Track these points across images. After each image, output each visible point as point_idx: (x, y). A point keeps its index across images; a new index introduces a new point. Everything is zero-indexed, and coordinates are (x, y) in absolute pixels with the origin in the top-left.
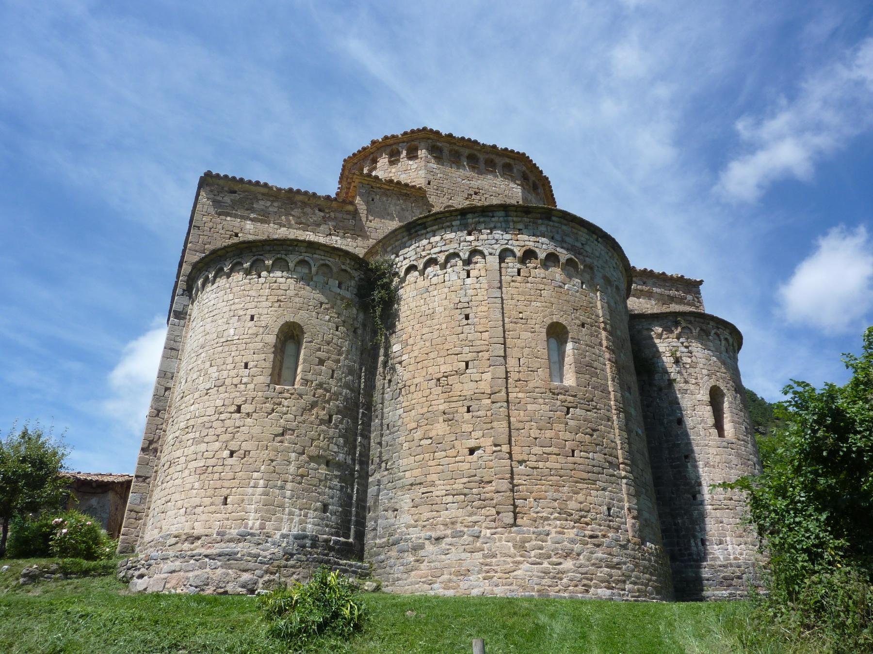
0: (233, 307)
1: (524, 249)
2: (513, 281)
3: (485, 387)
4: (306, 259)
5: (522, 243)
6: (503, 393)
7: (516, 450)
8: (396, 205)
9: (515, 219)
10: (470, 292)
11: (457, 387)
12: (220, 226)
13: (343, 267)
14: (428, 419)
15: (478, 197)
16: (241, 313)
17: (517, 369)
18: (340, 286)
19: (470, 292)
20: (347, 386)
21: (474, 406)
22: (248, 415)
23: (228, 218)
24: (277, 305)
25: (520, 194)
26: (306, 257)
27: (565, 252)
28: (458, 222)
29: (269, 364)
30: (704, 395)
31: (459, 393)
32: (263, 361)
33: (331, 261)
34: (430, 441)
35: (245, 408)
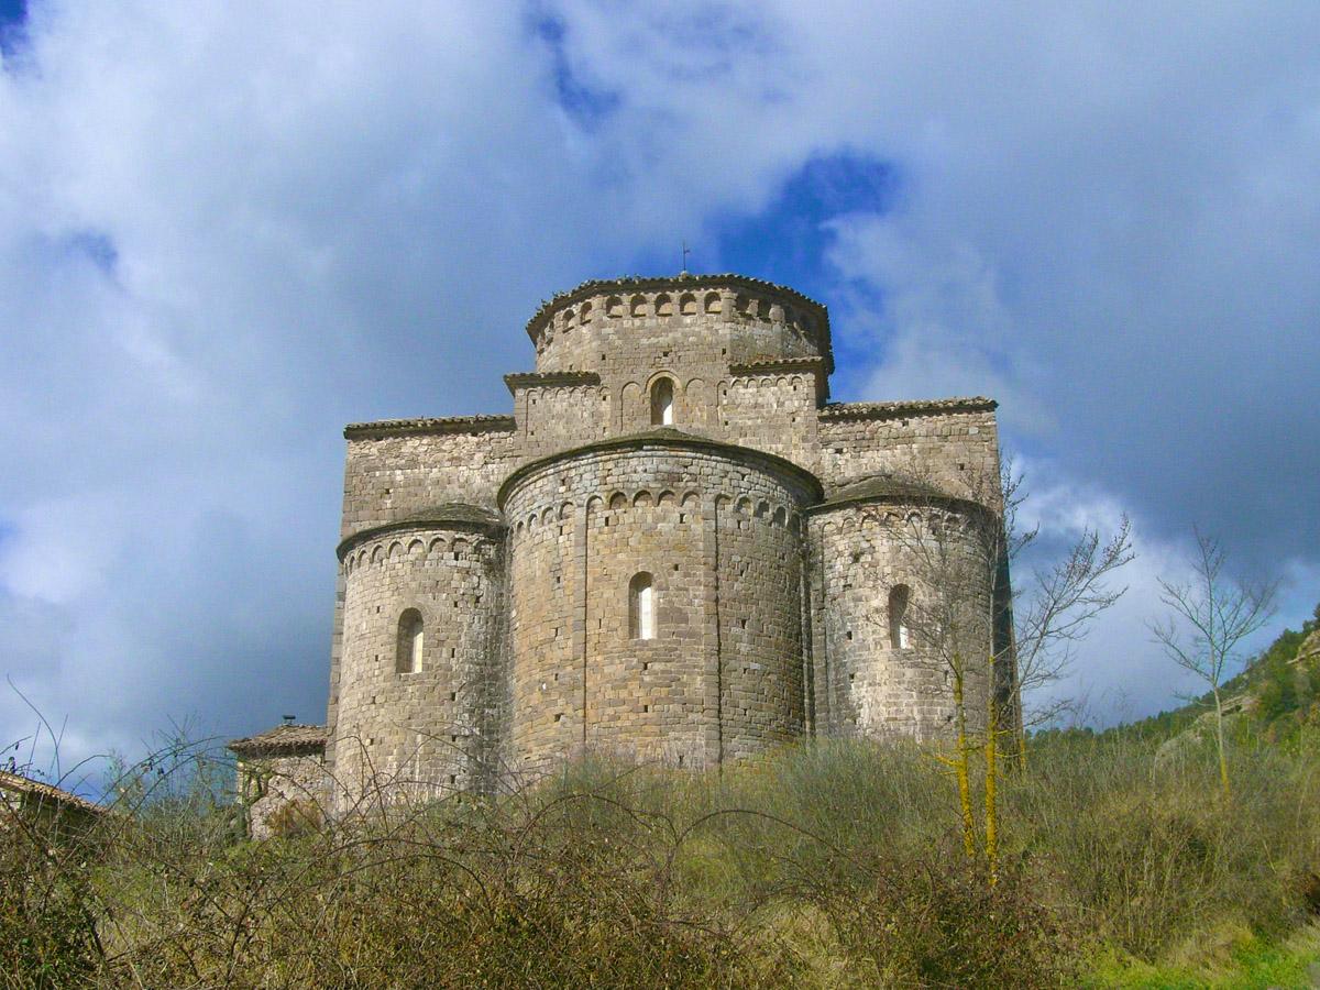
0: (365, 600)
1: (613, 493)
2: (600, 533)
3: (568, 653)
4: (418, 538)
5: (610, 487)
6: (582, 659)
7: (591, 712)
8: (562, 400)
9: (604, 458)
10: (562, 552)
11: (549, 655)
12: (370, 486)
13: (457, 536)
14: (529, 688)
15: (668, 359)
16: (370, 605)
17: (597, 631)
18: (456, 558)
19: (562, 552)
20: (470, 661)
21: (561, 673)
22: (382, 705)
23: (378, 474)
24: (396, 593)
25: (728, 337)
26: (418, 535)
27: (659, 485)
28: (552, 470)
29: (393, 655)
30: (880, 600)
31: (550, 661)
32: (388, 652)
33: (442, 534)
34: (530, 709)
35: (378, 700)
